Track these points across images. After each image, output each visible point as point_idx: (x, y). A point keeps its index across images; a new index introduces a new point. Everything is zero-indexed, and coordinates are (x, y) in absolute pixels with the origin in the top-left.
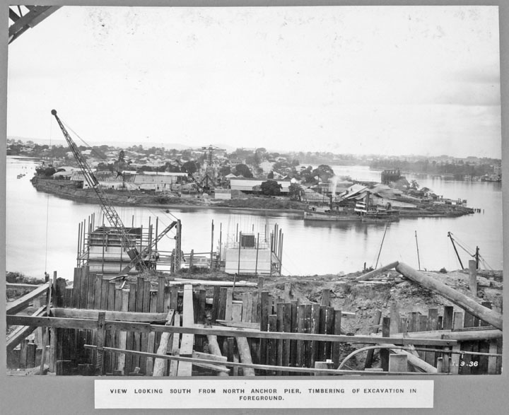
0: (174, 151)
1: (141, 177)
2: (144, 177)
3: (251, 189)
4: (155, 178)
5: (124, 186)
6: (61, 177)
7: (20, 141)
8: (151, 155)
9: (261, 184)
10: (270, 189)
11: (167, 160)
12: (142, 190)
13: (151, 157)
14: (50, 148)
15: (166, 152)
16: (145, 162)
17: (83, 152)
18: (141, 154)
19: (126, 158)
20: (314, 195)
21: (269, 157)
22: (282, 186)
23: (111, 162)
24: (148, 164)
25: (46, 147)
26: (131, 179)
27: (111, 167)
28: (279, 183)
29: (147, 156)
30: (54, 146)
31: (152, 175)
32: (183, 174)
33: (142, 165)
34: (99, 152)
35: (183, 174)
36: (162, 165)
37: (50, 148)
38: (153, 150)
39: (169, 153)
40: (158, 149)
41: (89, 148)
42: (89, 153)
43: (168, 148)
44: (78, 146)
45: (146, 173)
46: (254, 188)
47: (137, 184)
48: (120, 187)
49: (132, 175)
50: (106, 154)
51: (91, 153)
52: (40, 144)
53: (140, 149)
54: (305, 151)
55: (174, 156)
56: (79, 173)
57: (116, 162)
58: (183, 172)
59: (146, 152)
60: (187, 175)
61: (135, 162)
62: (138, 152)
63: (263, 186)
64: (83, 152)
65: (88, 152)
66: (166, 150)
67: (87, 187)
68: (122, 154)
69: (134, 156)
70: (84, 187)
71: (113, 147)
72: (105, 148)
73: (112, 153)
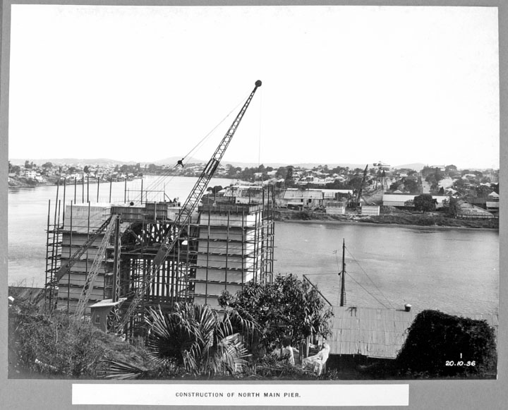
9: (413, 199)
10: (424, 203)
15: (350, 172)
17: (269, 173)
20: (471, 210)
22: (438, 201)
25: (239, 169)
28: (434, 197)
30: (247, 168)
41: (275, 170)
44: (266, 167)
46: (407, 202)
47: (287, 200)
59: (329, 172)
60: (351, 192)
64: (269, 173)
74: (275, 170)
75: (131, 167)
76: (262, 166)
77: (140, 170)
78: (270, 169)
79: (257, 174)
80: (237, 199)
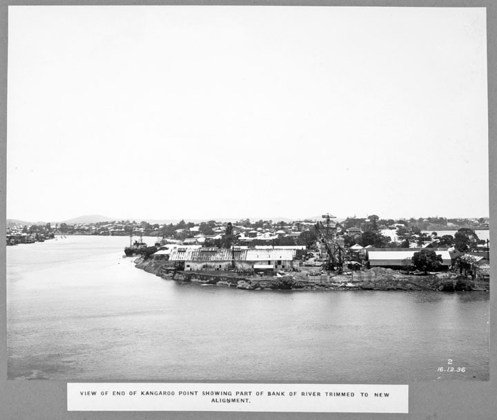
0: (282, 223)
1: (254, 252)
2: (259, 253)
3: (400, 264)
4: (270, 253)
5: (233, 266)
6: (163, 256)
7: (134, 222)
8: (259, 229)
10: (426, 263)
12: (257, 271)
13: (259, 231)
14: (160, 227)
15: (275, 225)
16: (255, 235)
17: (192, 229)
18: (248, 228)
19: (235, 232)
21: (389, 224)
22: (443, 258)
23: (218, 237)
24: (260, 237)
25: (157, 226)
26: (242, 255)
27: (218, 244)
31: (268, 250)
32: (300, 248)
33: (252, 239)
34: (207, 228)
35: (300, 248)
36: (271, 238)
38: (260, 224)
40: (265, 222)
41: (197, 225)
42: (198, 230)
43: (275, 222)
44: (187, 223)
45: (257, 247)
48: (229, 265)
49: (243, 251)
50: (213, 229)
51: (200, 229)
52: (152, 224)
53: (247, 224)
54: (417, 218)
56: (180, 251)
57: (223, 236)
58: (299, 245)
60: (304, 248)
61: (246, 236)
62: (245, 226)
63: (415, 258)
64: (192, 229)
65: (196, 229)
66: (273, 223)
67: (189, 269)
68: (230, 227)
69: (242, 231)
70: (187, 269)
71: (220, 223)
72: (212, 224)
73: (220, 229)
74: (197, 225)
75: (40, 228)
76: (183, 222)
77: (51, 230)
78: (192, 225)
79: (179, 231)
80: (186, 264)
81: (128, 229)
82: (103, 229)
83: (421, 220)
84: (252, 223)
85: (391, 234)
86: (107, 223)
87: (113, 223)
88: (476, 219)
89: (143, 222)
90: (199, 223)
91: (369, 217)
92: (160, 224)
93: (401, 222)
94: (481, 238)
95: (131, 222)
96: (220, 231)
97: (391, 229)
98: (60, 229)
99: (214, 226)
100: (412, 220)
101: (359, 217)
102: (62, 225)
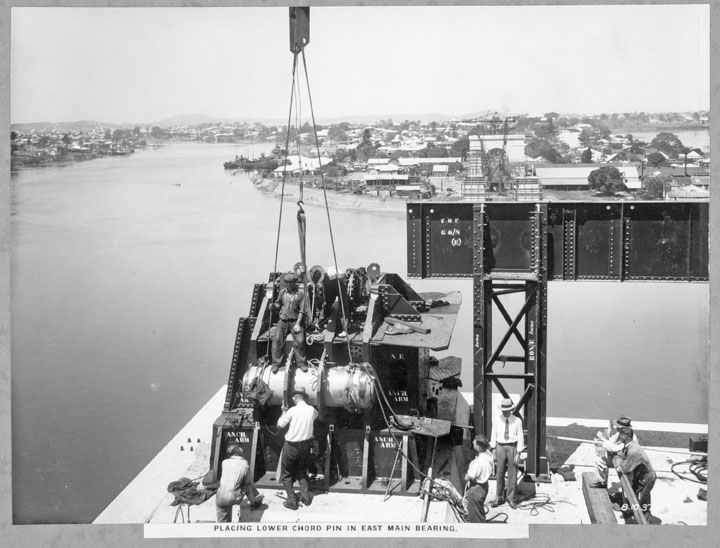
8: (404, 132)
11: (428, 139)
13: (404, 134)
14: (280, 130)
15: (424, 126)
16: (398, 144)
17: (318, 133)
19: (373, 138)
24: (403, 148)
29: (400, 133)
34: (339, 131)
37: (280, 130)
38: (405, 126)
39: (428, 127)
40: (412, 123)
41: (326, 128)
51: (329, 133)
53: (390, 125)
55: (434, 131)
66: (422, 124)
71: (355, 125)
72: (345, 126)
74: (326, 128)
75: (127, 132)
81: (239, 135)
82: (206, 133)
83: (615, 115)
84: (395, 124)
85: (570, 139)
86: (210, 125)
87: (219, 125)
88: (688, 114)
89: (257, 124)
90: (328, 124)
91: (546, 115)
92: (277, 125)
93: (586, 120)
94: (686, 144)
95: (242, 124)
96: (354, 135)
97: (572, 131)
98: (152, 134)
99: (347, 129)
100: (604, 116)
101: (532, 115)
102: (154, 129)
